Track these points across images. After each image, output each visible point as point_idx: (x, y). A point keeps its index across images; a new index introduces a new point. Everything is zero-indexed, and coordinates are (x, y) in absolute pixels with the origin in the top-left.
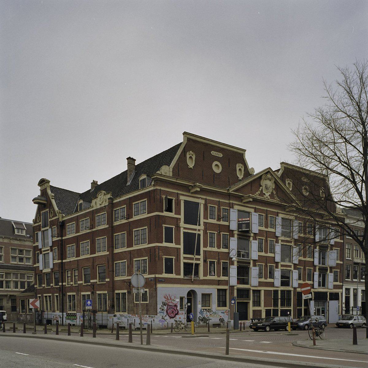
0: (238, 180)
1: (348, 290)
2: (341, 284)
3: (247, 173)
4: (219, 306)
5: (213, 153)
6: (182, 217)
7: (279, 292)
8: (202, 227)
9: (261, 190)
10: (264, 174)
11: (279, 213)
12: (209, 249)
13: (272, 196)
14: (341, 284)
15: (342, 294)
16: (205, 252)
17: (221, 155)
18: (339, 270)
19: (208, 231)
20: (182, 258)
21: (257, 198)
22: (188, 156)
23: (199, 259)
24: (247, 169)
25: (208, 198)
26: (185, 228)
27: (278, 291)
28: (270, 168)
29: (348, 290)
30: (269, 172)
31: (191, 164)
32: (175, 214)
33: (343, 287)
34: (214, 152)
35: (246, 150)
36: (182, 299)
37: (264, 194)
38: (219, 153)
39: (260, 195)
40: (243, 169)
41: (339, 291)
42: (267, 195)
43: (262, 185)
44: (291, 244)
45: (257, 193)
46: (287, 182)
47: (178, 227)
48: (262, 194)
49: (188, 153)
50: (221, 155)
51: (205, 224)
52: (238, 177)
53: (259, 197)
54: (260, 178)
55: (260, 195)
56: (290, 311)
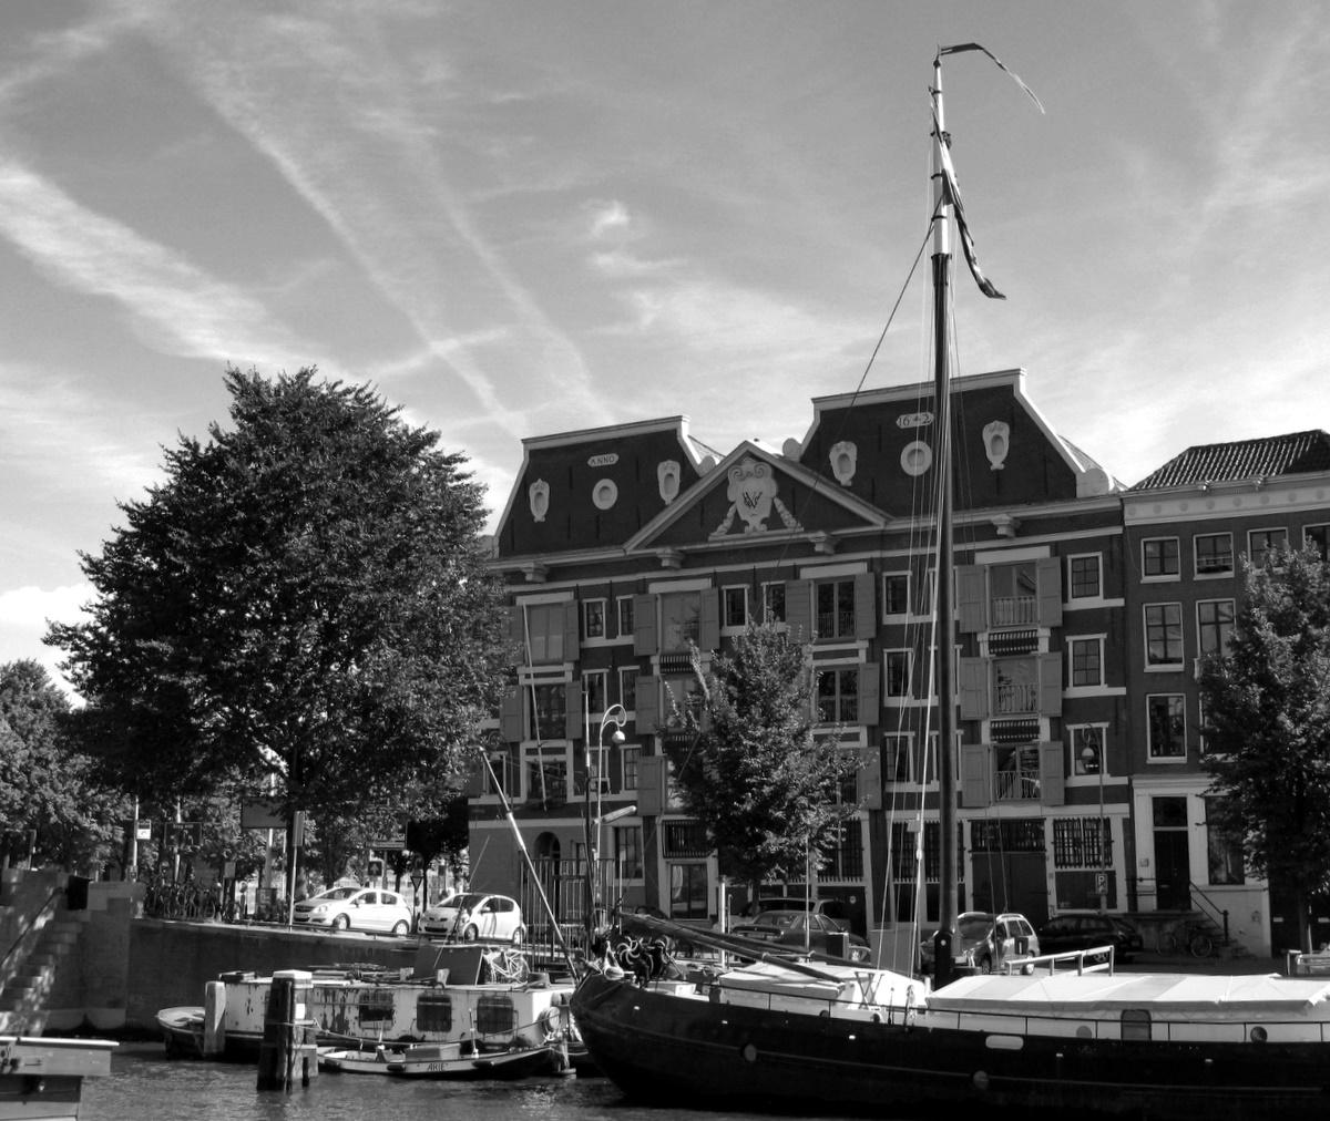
0: (662, 506)
1: (1170, 811)
2: (1123, 780)
3: (689, 475)
10: (733, 464)
13: (773, 521)
14: (1123, 780)
15: (1129, 825)
17: (613, 458)
18: (1104, 725)
24: (691, 466)
25: (719, 569)
29: (1170, 811)
31: (539, 511)
33: (1136, 792)
37: (746, 523)
39: (730, 531)
41: (1115, 812)
45: (720, 528)
48: (739, 525)
49: (532, 488)
50: (613, 458)
53: (736, 540)
54: (723, 484)
55: (730, 531)
56: (860, 892)
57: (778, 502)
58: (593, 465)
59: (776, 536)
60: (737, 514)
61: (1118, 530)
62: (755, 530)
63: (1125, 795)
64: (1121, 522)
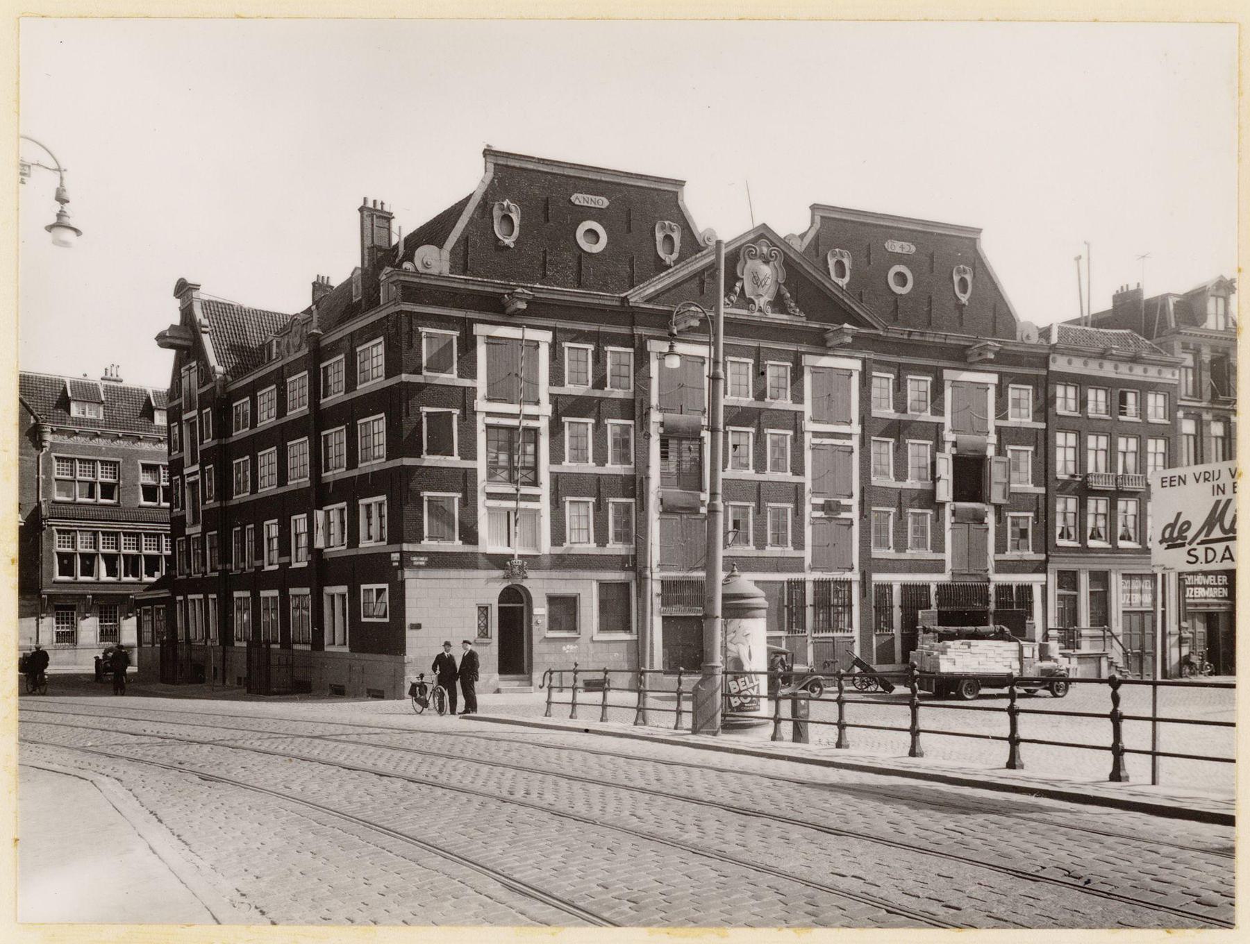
0: (661, 266)
3: (692, 244)
4: (604, 626)
5: (579, 199)
6: (481, 383)
7: (809, 588)
8: (546, 409)
9: (737, 289)
11: (804, 353)
12: (567, 466)
13: (778, 303)
15: (1045, 589)
16: (556, 478)
17: (603, 202)
19: (564, 419)
20: (481, 498)
21: (738, 317)
22: (497, 213)
23: (536, 498)
26: (489, 414)
27: (801, 584)
28: (764, 224)
30: (762, 236)
32: (460, 376)
33: (1050, 566)
34: (580, 196)
35: (685, 182)
36: (484, 610)
38: (598, 198)
40: (676, 237)
41: (1036, 580)
42: (762, 302)
43: (741, 276)
44: (848, 443)
46: (831, 262)
47: (468, 415)
48: (747, 302)
50: (603, 202)
51: (554, 399)
52: (662, 260)
57: (783, 287)
58: (577, 203)
59: (783, 318)
60: (742, 289)
61: (1044, 372)
62: (760, 310)
63: (1041, 568)
64: (1047, 366)
